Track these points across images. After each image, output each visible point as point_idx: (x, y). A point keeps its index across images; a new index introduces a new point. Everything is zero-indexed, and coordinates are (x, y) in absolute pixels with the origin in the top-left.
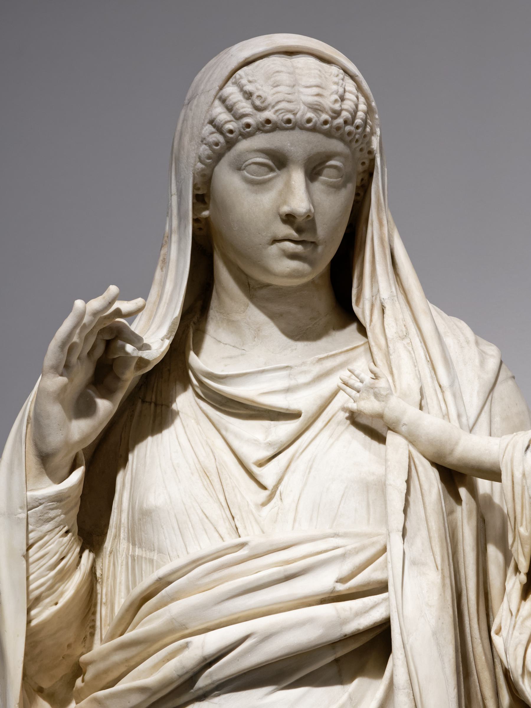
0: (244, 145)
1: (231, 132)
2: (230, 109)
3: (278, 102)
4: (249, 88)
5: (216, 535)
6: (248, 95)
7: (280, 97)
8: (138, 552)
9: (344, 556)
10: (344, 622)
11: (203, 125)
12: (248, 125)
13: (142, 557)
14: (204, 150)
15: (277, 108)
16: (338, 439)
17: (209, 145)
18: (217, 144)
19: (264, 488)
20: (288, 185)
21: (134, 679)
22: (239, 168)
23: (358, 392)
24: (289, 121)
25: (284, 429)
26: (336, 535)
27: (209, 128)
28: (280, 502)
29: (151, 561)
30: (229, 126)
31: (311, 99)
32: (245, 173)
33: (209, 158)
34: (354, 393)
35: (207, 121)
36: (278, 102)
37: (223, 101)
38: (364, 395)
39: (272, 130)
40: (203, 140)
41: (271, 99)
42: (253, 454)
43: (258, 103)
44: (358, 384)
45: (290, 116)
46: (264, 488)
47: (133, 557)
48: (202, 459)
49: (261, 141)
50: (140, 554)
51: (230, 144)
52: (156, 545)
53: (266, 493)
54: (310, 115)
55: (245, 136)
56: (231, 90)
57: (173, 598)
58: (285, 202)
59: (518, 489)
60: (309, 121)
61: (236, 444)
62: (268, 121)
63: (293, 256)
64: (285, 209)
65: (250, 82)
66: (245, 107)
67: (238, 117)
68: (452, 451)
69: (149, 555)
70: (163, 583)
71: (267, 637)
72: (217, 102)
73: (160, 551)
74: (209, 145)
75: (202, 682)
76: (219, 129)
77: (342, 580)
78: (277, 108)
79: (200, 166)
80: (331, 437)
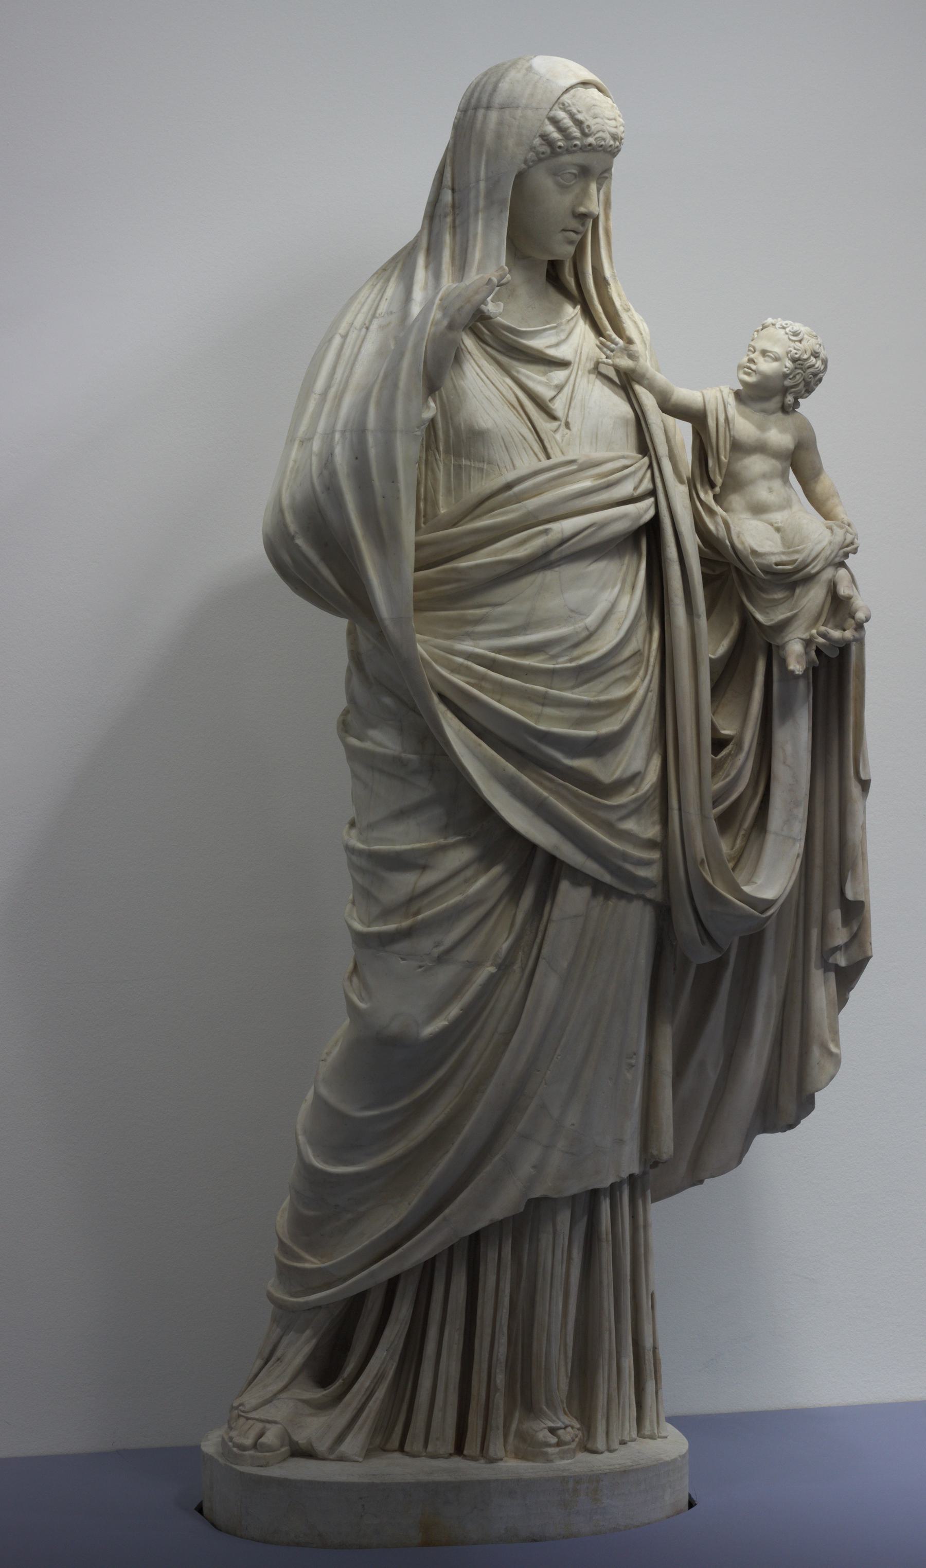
0: (566, 158)
1: (560, 147)
2: (562, 130)
3: (598, 132)
4: (580, 117)
5: (531, 452)
6: (579, 123)
7: (599, 127)
8: (464, 462)
9: (634, 473)
10: (640, 516)
11: (535, 137)
12: (575, 146)
13: (470, 466)
14: (531, 155)
15: (597, 136)
16: (594, 385)
17: (537, 153)
18: (543, 153)
19: (554, 418)
20: (585, 192)
21: (489, 555)
22: (555, 173)
23: (612, 351)
24: (602, 146)
25: (559, 375)
26: (623, 457)
28: (567, 431)
29: (481, 470)
30: (560, 144)
31: (613, 130)
32: (559, 178)
33: (533, 161)
34: (608, 352)
36: (598, 132)
38: (619, 354)
39: (590, 151)
41: (594, 128)
42: (546, 393)
43: (587, 131)
44: (613, 346)
45: (603, 143)
46: (554, 418)
47: (460, 466)
48: (505, 393)
49: (579, 158)
50: (468, 463)
52: (486, 458)
53: (555, 424)
54: (612, 142)
55: (568, 151)
56: (561, 115)
57: (519, 498)
58: (581, 204)
59: (721, 430)
60: (611, 146)
61: (530, 384)
62: (590, 145)
63: (571, 242)
64: (582, 210)
65: (579, 112)
66: (576, 132)
68: (670, 399)
69: (477, 464)
70: (509, 486)
71: (603, 525)
72: (547, 122)
73: (489, 463)
74: (537, 153)
75: (554, 556)
77: (635, 488)
78: (597, 136)
79: (523, 166)
80: (588, 382)
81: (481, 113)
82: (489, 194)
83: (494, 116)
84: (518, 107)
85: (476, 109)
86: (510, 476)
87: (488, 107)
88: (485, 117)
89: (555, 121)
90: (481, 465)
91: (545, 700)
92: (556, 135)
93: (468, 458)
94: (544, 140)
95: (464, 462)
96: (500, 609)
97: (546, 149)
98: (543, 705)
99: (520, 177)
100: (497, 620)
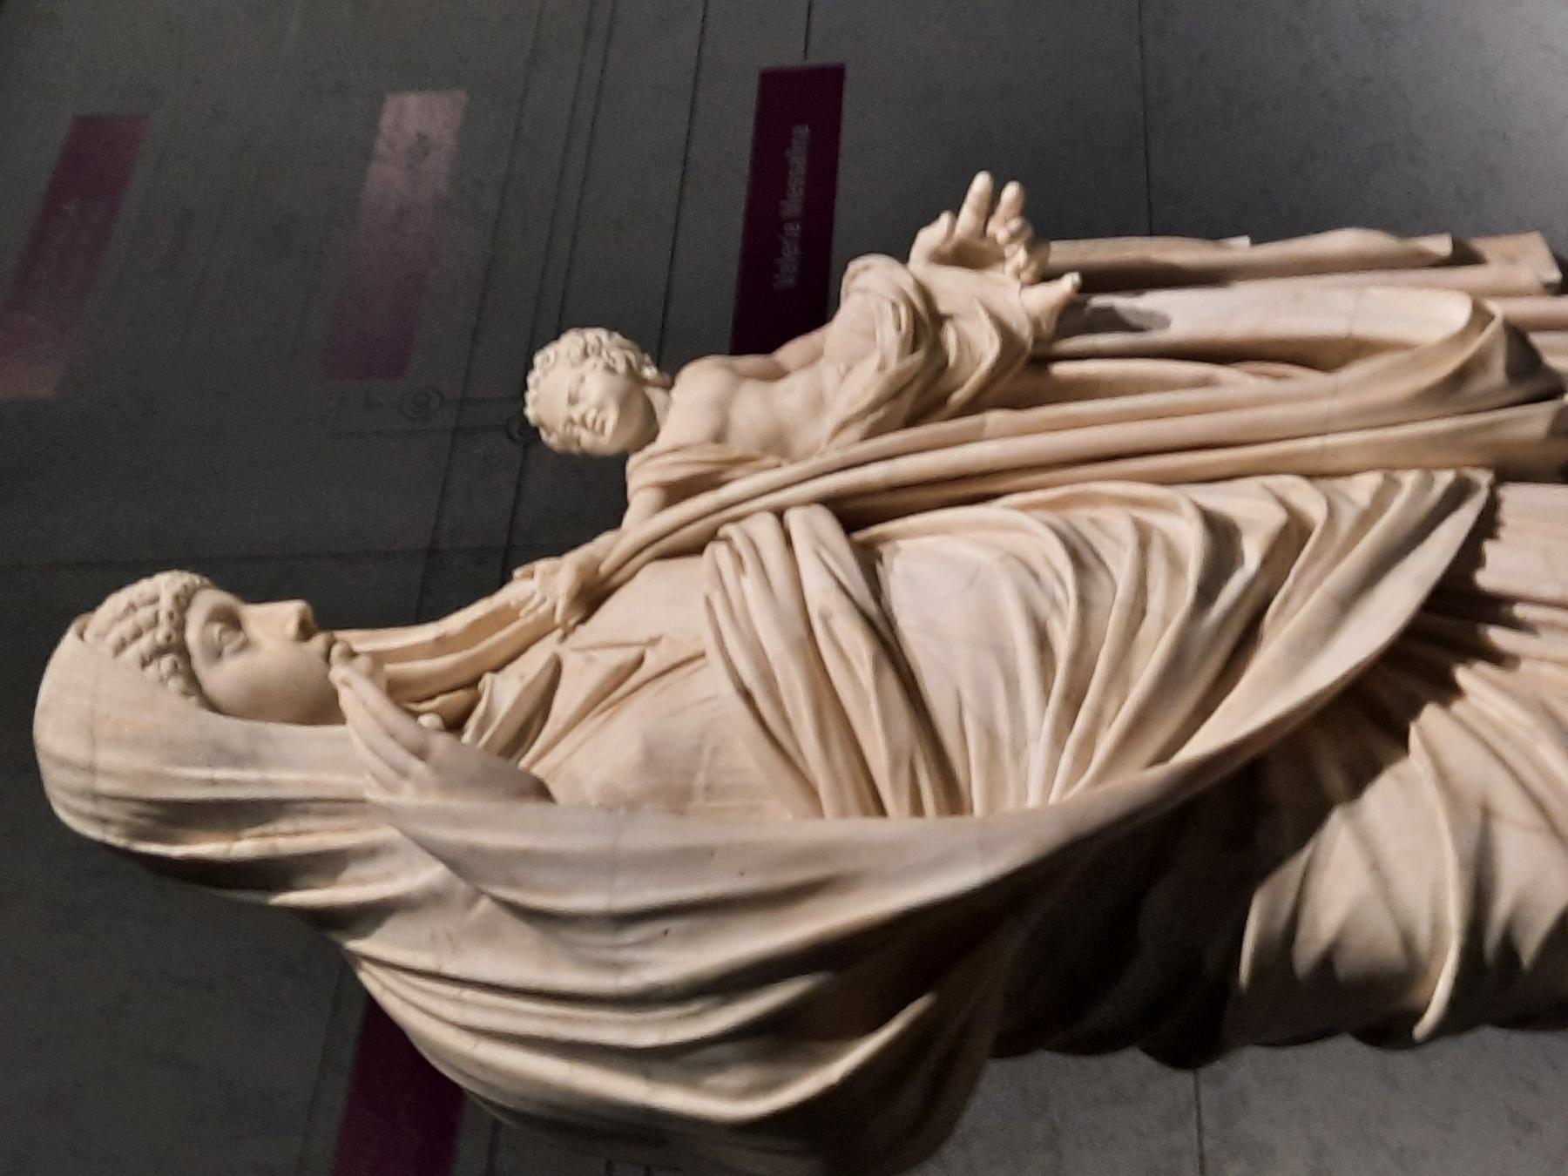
1: (169, 638)
2: (138, 635)
8: (700, 779)
14: (175, 684)
18: (176, 666)
27: (151, 669)
29: (715, 750)
35: (139, 670)
37: (122, 646)
40: (162, 681)
47: (709, 789)
51: (182, 651)
67: (155, 622)
76: (159, 652)
81: (105, 785)
82: (237, 760)
83: (107, 757)
84: (92, 713)
85: (96, 797)
86: (727, 689)
87: (91, 769)
88: (110, 774)
89: (122, 646)
90: (707, 750)
91: (1138, 611)
92: (145, 644)
93: (690, 774)
94: (151, 660)
95: (700, 779)
96: (967, 696)
97: (166, 662)
98: (1143, 613)
99: (212, 706)
100: (986, 700)
